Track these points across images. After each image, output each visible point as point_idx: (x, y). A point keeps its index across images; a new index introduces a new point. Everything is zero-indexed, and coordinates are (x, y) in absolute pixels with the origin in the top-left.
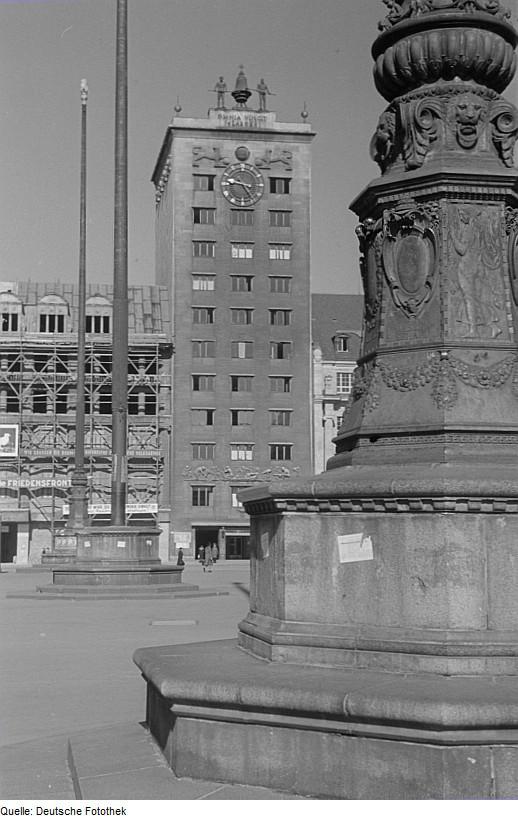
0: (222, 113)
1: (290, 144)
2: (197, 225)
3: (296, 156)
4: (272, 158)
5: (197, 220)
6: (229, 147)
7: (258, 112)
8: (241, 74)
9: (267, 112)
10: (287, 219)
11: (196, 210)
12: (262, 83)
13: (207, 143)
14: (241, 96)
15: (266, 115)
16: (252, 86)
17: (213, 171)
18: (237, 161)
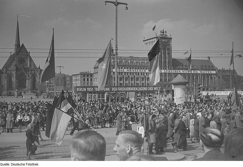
6: (162, 39)
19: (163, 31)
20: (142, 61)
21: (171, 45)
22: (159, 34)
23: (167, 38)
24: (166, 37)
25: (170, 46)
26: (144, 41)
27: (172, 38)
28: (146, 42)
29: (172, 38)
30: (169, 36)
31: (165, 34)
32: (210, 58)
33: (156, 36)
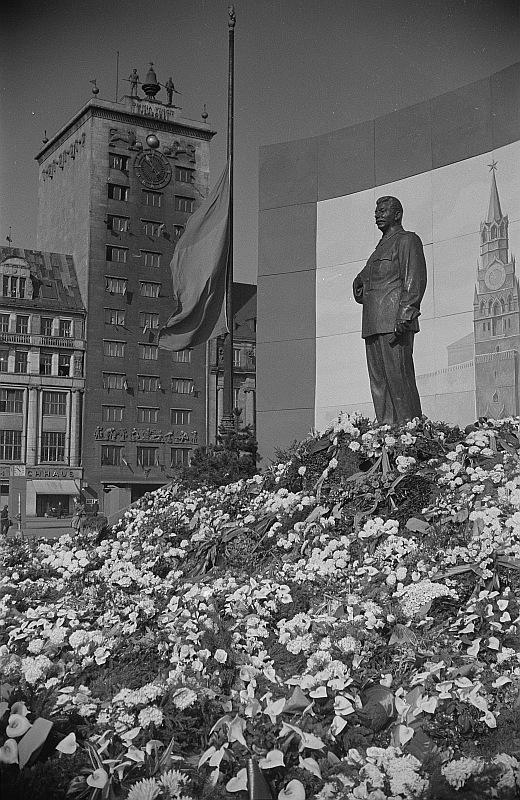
0: (136, 101)
2: (111, 201)
5: (110, 196)
6: (141, 132)
7: (167, 106)
8: (152, 70)
9: (173, 107)
10: (189, 206)
11: (111, 186)
12: (171, 81)
13: (123, 126)
14: (152, 90)
15: (173, 110)
16: (162, 81)
17: (127, 153)
18: (148, 148)
23: (176, 128)
24: (174, 119)
29: (208, 135)
31: (162, 95)
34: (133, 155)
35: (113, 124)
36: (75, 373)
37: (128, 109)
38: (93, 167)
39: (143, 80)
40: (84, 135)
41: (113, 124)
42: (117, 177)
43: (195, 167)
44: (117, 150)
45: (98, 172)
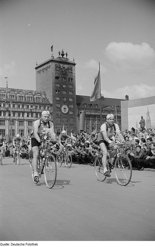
1: (72, 66)
3: (73, 68)
4: (69, 68)
6: (61, 65)
8: (63, 51)
13: (58, 64)
14: (63, 55)
16: (65, 53)
17: (59, 69)
19: (63, 52)
20: (29, 96)
21: (75, 73)
22: (56, 56)
23: (68, 64)
24: (68, 62)
25: (73, 75)
26: (36, 68)
27: (75, 64)
28: (39, 69)
29: (75, 64)
30: (71, 60)
31: (65, 56)
32: (128, 97)
33: (51, 60)
34: (60, 70)
35: (56, 64)
36: (51, 117)
37: (59, 60)
38: (52, 73)
39: (61, 53)
40: (50, 66)
41: (56, 64)
42: (57, 75)
43: (72, 72)
44: (57, 69)
45: (53, 74)
